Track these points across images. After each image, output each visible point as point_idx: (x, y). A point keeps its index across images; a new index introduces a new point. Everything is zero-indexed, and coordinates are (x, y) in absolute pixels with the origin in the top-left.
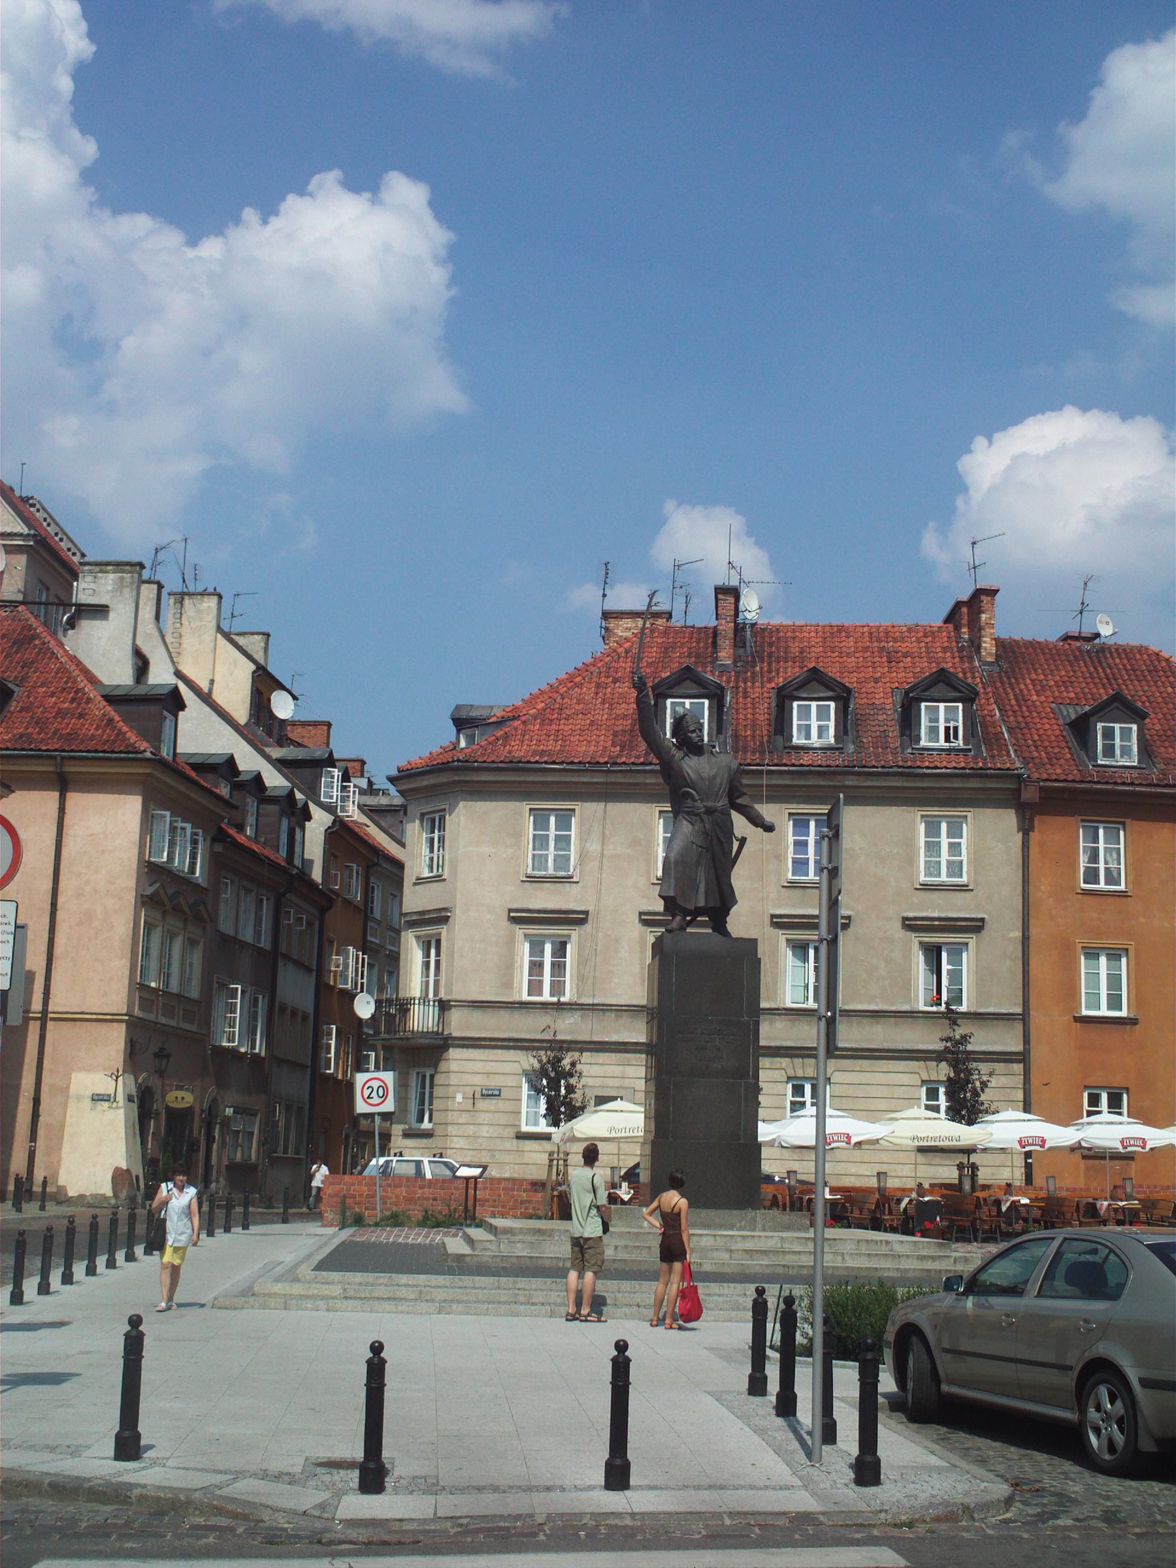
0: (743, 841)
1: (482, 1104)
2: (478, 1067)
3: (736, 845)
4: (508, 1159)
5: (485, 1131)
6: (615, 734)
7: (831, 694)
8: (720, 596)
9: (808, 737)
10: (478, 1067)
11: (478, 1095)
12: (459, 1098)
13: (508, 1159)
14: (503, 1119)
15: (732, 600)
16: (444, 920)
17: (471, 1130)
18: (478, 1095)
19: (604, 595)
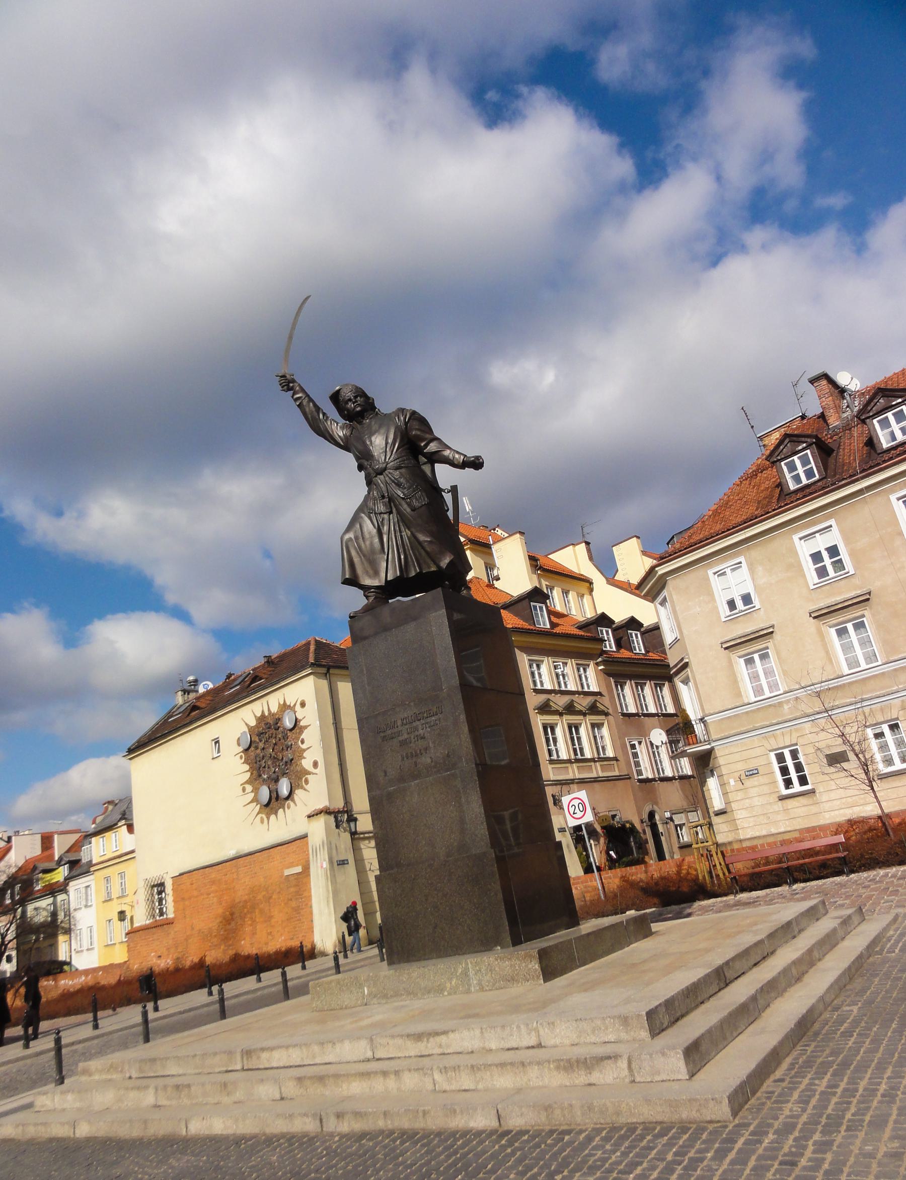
0: (454, 490)
1: (749, 783)
2: (737, 757)
3: (448, 498)
4: (779, 817)
5: (757, 801)
6: (759, 502)
7: (900, 400)
8: (816, 384)
9: (894, 438)
10: (737, 757)
11: (743, 777)
12: (732, 782)
13: (779, 817)
14: (766, 789)
15: (824, 382)
16: (686, 665)
17: (747, 802)
18: (743, 777)
19: (752, 427)
